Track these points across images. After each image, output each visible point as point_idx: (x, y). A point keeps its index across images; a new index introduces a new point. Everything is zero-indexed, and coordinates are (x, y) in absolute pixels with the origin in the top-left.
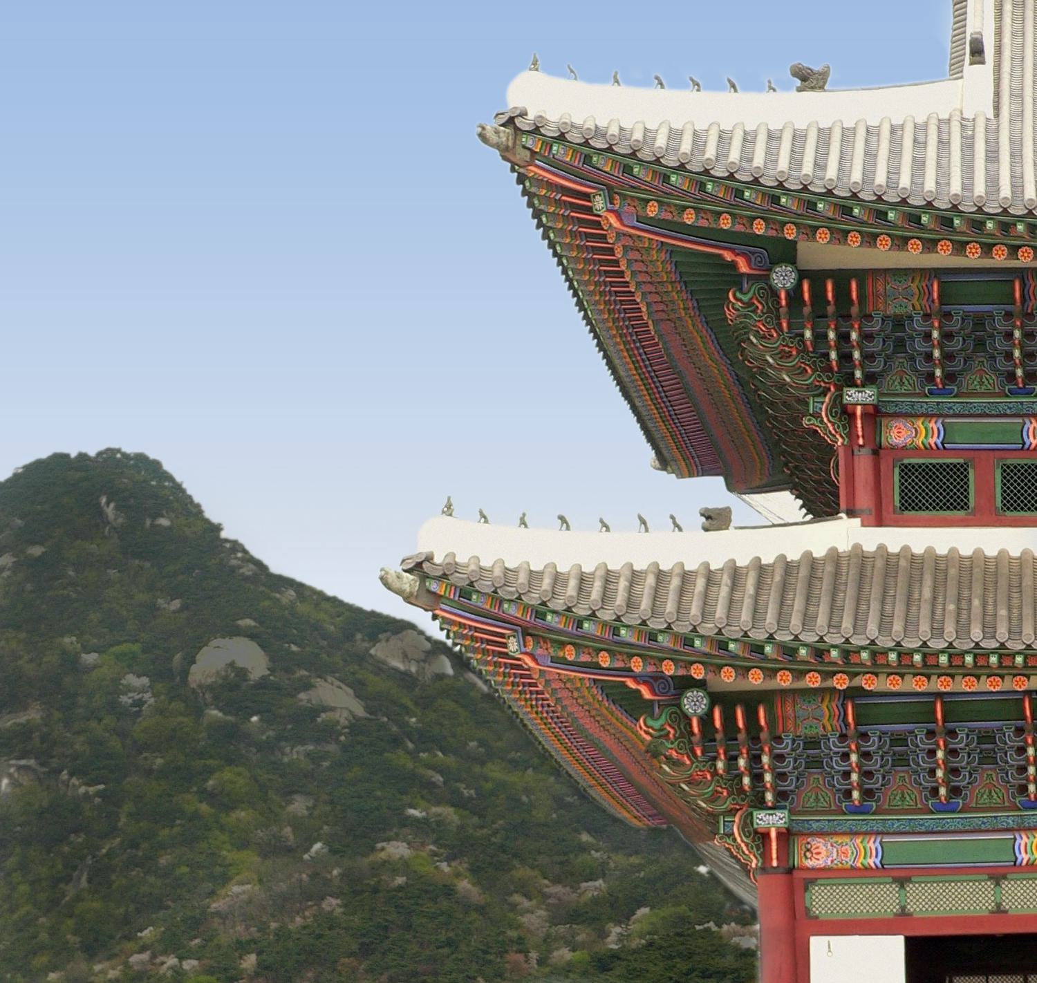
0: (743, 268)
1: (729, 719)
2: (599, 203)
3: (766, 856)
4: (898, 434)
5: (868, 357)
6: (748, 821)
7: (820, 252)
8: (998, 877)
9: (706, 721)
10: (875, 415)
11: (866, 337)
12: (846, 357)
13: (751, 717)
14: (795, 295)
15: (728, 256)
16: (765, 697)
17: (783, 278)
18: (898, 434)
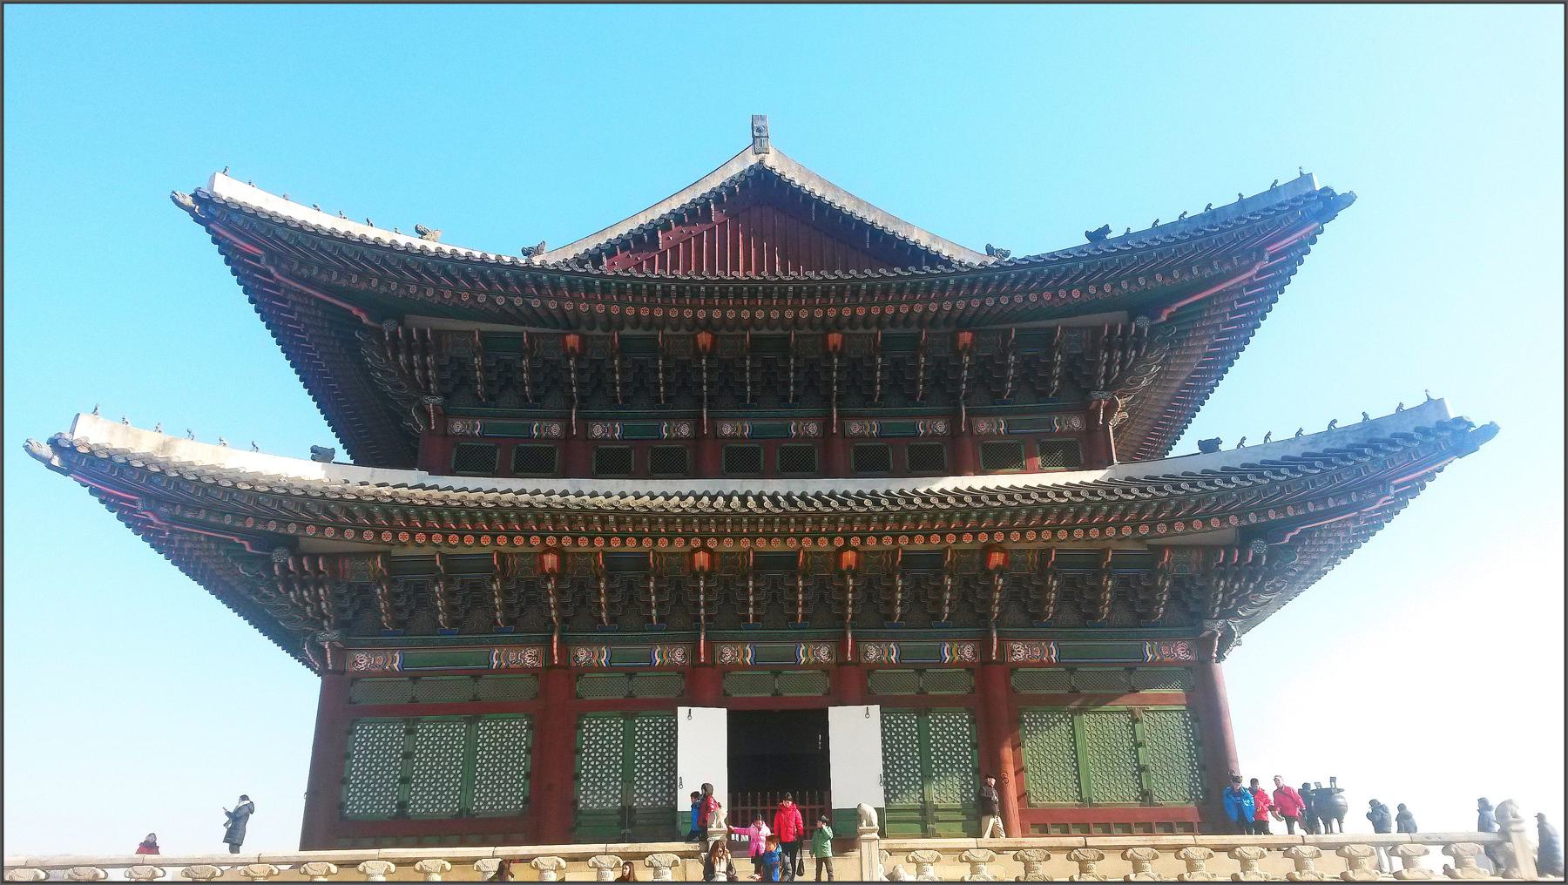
0: (365, 320)
1: (299, 565)
2: (263, 260)
3: (324, 663)
4: (458, 427)
5: (442, 382)
6: (315, 637)
7: (416, 321)
8: (476, 676)
9: (284, 567)
10: (445, 415)
11: (440, 368)
12: (428, 382)
13: (315, 565)
14: (394, 335)
15: (355, 312)
16: (333, 557)
17: (388, 327)
18: (458, 427)
